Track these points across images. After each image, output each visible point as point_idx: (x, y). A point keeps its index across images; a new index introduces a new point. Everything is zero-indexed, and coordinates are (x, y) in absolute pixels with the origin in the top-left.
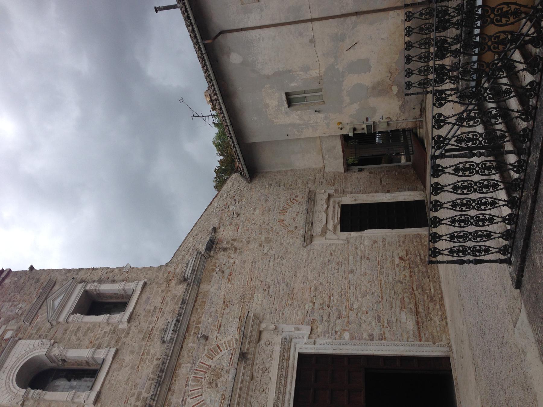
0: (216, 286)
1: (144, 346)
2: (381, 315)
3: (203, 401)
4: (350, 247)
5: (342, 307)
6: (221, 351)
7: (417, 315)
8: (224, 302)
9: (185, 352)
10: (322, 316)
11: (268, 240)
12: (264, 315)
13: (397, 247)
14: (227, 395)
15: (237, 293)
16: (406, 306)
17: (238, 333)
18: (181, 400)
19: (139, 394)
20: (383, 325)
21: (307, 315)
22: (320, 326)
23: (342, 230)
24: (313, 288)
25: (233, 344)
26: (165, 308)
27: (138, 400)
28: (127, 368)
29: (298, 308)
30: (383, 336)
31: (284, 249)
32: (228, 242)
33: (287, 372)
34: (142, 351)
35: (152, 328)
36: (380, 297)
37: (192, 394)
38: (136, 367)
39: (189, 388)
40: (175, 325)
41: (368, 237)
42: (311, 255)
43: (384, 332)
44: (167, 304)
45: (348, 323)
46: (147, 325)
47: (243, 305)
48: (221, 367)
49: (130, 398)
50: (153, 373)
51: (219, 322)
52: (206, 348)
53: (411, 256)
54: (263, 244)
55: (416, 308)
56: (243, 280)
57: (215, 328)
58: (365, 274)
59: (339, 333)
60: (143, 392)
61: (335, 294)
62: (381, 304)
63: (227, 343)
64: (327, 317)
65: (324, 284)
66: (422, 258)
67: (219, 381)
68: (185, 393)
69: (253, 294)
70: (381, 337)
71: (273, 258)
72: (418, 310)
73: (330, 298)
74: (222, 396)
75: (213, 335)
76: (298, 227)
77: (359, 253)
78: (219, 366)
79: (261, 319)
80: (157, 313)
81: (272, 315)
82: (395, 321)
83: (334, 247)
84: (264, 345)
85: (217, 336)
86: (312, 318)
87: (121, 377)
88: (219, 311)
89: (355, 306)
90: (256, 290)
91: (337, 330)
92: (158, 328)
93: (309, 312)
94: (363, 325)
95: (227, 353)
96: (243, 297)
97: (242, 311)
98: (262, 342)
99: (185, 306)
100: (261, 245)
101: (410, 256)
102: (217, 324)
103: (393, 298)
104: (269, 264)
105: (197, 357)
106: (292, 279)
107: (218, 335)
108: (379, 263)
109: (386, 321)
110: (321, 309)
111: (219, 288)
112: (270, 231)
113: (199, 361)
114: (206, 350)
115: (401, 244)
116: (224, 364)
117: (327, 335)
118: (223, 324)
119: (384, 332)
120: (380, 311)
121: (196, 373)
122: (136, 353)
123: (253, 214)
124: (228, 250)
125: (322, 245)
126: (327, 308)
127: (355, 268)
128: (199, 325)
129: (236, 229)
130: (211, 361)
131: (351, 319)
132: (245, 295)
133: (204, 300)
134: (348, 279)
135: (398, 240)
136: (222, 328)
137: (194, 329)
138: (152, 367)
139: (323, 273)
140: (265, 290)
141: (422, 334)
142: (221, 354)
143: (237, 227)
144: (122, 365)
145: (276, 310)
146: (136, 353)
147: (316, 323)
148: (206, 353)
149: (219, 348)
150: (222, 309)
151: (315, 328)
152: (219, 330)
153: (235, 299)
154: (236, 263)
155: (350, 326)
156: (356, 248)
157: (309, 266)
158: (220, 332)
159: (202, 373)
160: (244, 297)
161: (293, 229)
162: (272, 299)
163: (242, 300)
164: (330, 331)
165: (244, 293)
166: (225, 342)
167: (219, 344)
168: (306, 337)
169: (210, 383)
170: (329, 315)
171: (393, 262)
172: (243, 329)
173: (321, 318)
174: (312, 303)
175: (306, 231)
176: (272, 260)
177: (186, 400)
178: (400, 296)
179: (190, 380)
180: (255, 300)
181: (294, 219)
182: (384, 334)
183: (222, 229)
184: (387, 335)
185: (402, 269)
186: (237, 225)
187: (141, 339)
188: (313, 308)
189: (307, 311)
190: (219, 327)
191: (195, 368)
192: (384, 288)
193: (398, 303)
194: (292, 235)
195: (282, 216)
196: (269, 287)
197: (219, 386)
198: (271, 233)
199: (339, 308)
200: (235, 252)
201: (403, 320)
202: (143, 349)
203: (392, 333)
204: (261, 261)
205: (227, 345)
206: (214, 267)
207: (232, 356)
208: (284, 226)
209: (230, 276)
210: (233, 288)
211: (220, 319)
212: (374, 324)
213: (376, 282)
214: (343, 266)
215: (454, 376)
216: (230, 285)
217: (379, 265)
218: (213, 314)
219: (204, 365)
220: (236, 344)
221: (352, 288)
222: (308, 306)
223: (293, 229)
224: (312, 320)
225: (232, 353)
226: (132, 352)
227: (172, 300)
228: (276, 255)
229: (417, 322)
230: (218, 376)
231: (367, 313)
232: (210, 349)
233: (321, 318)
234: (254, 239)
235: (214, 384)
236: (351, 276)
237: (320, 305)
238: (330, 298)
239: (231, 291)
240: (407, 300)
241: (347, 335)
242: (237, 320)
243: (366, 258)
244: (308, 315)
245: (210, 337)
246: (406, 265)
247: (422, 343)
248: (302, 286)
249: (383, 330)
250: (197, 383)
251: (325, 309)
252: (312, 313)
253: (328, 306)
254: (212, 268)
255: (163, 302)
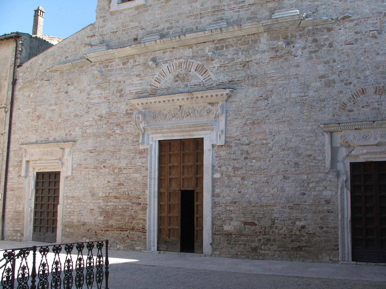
0: (265, 48)
1: (208, 11)
2: (237, 205)
3: (166, 75)
4: (319, 175)
5: (245, 170)
6: (202, 75)
7: (237, 235)
8: (248, 62)
9: (201, 46)
10: (234, 154)
11: (329, 84)
12: (235, 101)
13: (320, 225)
14: (170, 91)
15: (259, 71)
16: (247, 226)
17: (218, 83)
18: (166, 59)
19: (171, 28)
20: (227, 206)
21: (236, 140)
22: (225, 153)
23: (354, 166)
24: (264, 142)
25: (208, 83)
26: (243, 10)
27: (169, 28)
28: (190, 8)
29: (242, 131)
30: (217, 205)
31: (315, 104)
32: (327, 39)
33: (186, 131)
34: (204, 12)
35: (223, 9)
36: (256, 204)
37: (170, 66)
38: (191, 15)
39: (175, 62)
40: (216, 29)
41: (337, 193)
42: (307, 135)
43: (221, 206)
44: (248, 10)
45: (229, 177)
46: (225, 4)
47: (245, 80)
48: (189, 80)
49: (169, 23)
50: (187, 29)
51: (227, 65)
52: (205, 62)
53: (307, 238)
54: (323, 80)
55: (244, 235)
56: (274, 71)
57: (222, 62)
58: (283, 190)
59: (219, 169)
60: (174, 30)
61: (258, 164)
62: (248, 205)
63: (209, 77)
64: (234, 157)
65: (270, 152)
66: (303, 249)
67: (179, 82)
68: (171, 60)
69: (257, 86)
70: (216, 203)
71: (302, 94)
72: (243, 236)
73: (254, 158)
74: (169, 88)
75: (216, 64)
76: (352, 113)
77: (311, 185)
78: (190, 78)
79: (230, 100)
80: (239, 6)
81: (236, 109)
82: (233, 215)
83: (320, 158)
84: (207, 109)
85: (215, 67)
86: (233, 145)
87: (183, 7)
88: (240, 60)
89: (246, 182)
90: (261, 88)
91: (222, 168)
92: (224, 14)
93: (238, 142)
94: (227, 190)
95: (200, 81)
96: (253, 77)
97: (238, 80)
98: (210, 106)
99: (237, 29)
100: (322, 77)
101: (307, 236)
102: (227, 62)
103: (254, 216)
104: (293, 93)
105: (197, 58)
106: (275, 120)
107: (216, 68)
108: (296, 205)
109: (232, 208)
110: (242, 152)
111: (264, 52)
112: (345, 82)
113: (193, 61)
114: (202, 63)
115: (325, 229)
116: (192, 81)
117: (217, 159)
118: (226, 68)
119: (221, 206)
120: (240, 204)
121: (184, 62)
122: (202, 8)
123: (378, 54)
124: (315, 44)
125: (323, 145)
126: (243, 157)
127: (290, 181)
128: (225, 49)
129: (349, 40)
130: (194, 70)
131: (234, 179)
132: (256, 78)
133: (250, 42)
134: (276, 175)
135: (330, 226)
136: (222, 69)
137: (221, 45)
138: (192, 26)
139: (284, 150)
140: (262, 96)
141: (219, 236)
142: (199, 76)
143: (353, 42)
144: (192, 3)
145: (240, 112)
146: (202, 8)
147: (228, 148)
148: (200, 63)
149: (205, 73)
150: (241, 62)
151: (223, 149)
152: (220, 67)
153: (252, 71)
154: (296, 58)
155: (226, 178)
156: (318, 182)
157: (292, 134)
158: (218, 68)
159: (185, 67)
160: (254, 77)
161: (348, 108)
162: (252, 105)
163: (250, 78)
164: (221, 161)
165: (258, 77)
166: (210, 75)
167: (208, 71)
168: (215, 143)
169: (178, 76)
170: (235, 159)
171: (300, 220)
172: (221, 87)
173: (232, 153)
174: (248, 143)
175: (341, 125)
176: (300, 94)
177: (167, 63)
178: (256, 223)
179: (180, 60)
180: (251, 90)
181: (368, 106)
182: (219, 206)
183: (348, 25)
184: (219, 209)
185: (289, 227)
186: (356, 40)
187: (214, 5)
188: (243, 145)
189: (239, 140)
190: (223, 66)
191: (189, 60)
192: (265, 209)
193: (250, 220)
194: (338, 109)
195: (373, 90)
196: (265, 99)
197: (176, 83)
198: (343, 84)
199: (244, 168)
200: (311, 52)
201: (232, 223)
202: (205, 11)
203: (220, 212)
204: (298, 84)
205: (207, 78)
206: (289, 38)
207: (198, 85)
208: (353, 98)
209: (279, 57)
210: (264, 65)
211: (231, 64)
212: (228, 198)
213: (273, 201)
214: (293, 169)
215: (187, 253)
216: (268, 60)
217: (294, 205)
218: (235, 56)
219: (191, 66)
220: (208, 86)
221: (266, 179)
222: (245, 140)
223: (348, 108)
224: (231, 145)
225: (200, 85)
226: (202, 5)
227: (252, 13)
228: (307, 97)
229: (231, 234)
230: (183, 80)
231: (239, 192)
232: (204, 66)
233: (232, 153)
234: (333, 67)
235: (177, 79)
236: (281, 177)
237: (246, 150)
238: (254, 158)
239: (261, 64)
240: (253, 228)
241: (217, 176)
242: (230, 79)
243: (303, 192)
244: (235, 141)
245: (214, 62)
246: (293, 231)
247: (210, 235)
248: (267, 131)
249: (223, 205)
250: (178, 66)
251: (242, 156)
252: (237, 145)
253: (246, 158)
254: (288, 36)
255: (249, 6)
